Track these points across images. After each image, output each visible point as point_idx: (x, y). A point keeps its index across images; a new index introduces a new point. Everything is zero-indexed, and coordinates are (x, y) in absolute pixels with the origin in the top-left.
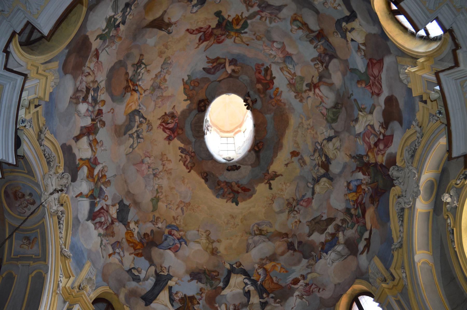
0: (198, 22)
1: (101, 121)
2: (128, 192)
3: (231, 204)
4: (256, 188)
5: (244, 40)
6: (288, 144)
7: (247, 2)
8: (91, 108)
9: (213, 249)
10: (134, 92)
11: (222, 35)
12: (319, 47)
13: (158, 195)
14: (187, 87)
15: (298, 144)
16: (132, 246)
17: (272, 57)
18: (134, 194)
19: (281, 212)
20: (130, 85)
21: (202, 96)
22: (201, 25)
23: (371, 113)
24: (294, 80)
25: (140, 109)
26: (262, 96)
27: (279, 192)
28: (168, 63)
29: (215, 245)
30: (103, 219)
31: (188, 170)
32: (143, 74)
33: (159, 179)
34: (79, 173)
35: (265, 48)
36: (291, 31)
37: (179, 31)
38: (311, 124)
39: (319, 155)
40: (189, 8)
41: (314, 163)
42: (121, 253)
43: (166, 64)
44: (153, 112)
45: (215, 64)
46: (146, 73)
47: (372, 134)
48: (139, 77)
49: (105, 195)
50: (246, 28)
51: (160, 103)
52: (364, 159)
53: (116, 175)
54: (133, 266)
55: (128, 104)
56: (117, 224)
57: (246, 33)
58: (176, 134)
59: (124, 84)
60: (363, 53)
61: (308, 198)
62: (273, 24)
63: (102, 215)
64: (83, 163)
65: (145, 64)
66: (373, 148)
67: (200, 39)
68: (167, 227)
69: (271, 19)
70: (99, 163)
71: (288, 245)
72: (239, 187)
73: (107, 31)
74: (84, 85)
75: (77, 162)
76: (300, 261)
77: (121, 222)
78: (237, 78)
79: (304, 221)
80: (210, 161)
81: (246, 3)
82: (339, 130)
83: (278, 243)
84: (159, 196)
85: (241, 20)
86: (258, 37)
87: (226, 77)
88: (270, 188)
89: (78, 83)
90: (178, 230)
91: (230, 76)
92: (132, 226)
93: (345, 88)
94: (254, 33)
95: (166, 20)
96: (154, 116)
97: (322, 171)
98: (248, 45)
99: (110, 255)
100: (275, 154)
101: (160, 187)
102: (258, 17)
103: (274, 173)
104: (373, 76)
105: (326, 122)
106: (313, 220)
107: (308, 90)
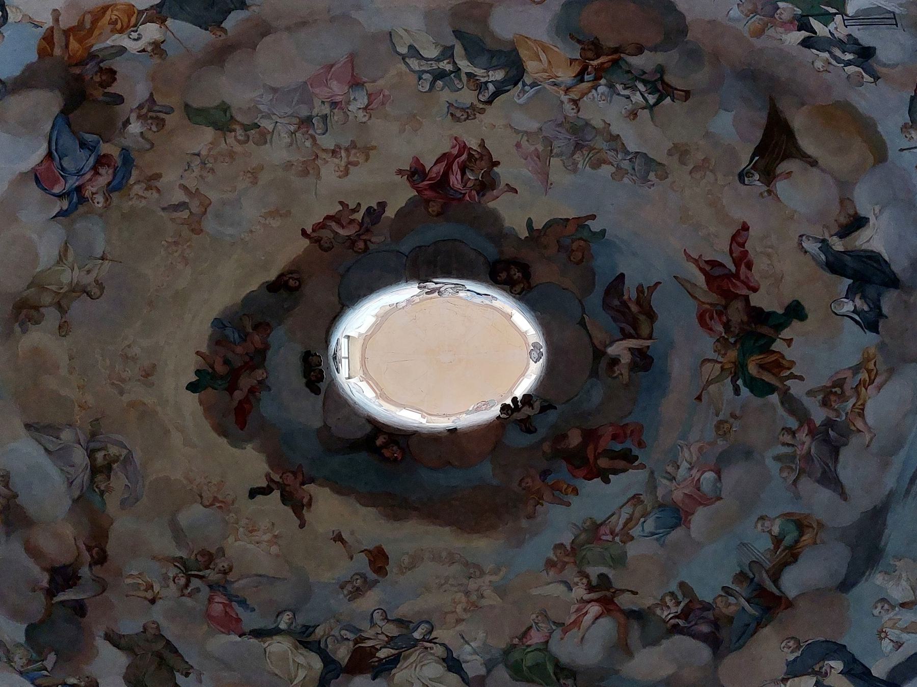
0: (769, 256)
2: (264, 29)
3: (193, 369)
4: (249, 447)
5: (712, 388)
6: (406, 537)
7: (838, 390)
9: (36, 308)
10: (577, 68)
11: (727, 326)
12: (732, 600)
13: (237, 127)
14: (571, 228)
15: (412, 566)
16: (81, 23)
17: (670, 469)
18: (254, 48)
19: (178, 534)
20: (602, 59)
21: (542, 273)
22: (760, 265)
24: (609, 538)
25: (524, 85)
26: (546, 447)
27: (243, 522)
29: (51, 317)
31: (309, 231)
32: (628, 97)
35: (694, 449)
36: (762, 518)
37: (744, 205)
38: (484, 602)
39: (391, 639)
40: (818, 232)
41: (365, 625)
43: (647, 167)
45: (634, 308)
46: (630, 107)
48: (619, 87)
50: (752, 391)
51: (532, 148)
54: (11, 17)
55: (545, 49)
57: (737, 391)
58: (428, 194)
59: (610, 41)
61: (239, 620)
62: (774, 467)
65: (656, 104)
67: (714, 264)
69: (792, 457)
71: (65, 567)
72: (252, 391)
76: (15, 614)
78: (594, 373)
79: (157, 613)
80: (335, 299)
83: (69, 531)
84: (234, 130)
86: (726, 426)
87: (596, 342)
88: (254, 493)
90: (111, 189)
91: (598, 354)
92: (151, 32)
94: (738, 413)
97: (343, 654)
98: (699, 398)
100: (370, 499)
101: (264, 138)
102: (793, 423)
103: (305, 501)
106: (168, 642)
107: (589, 582)
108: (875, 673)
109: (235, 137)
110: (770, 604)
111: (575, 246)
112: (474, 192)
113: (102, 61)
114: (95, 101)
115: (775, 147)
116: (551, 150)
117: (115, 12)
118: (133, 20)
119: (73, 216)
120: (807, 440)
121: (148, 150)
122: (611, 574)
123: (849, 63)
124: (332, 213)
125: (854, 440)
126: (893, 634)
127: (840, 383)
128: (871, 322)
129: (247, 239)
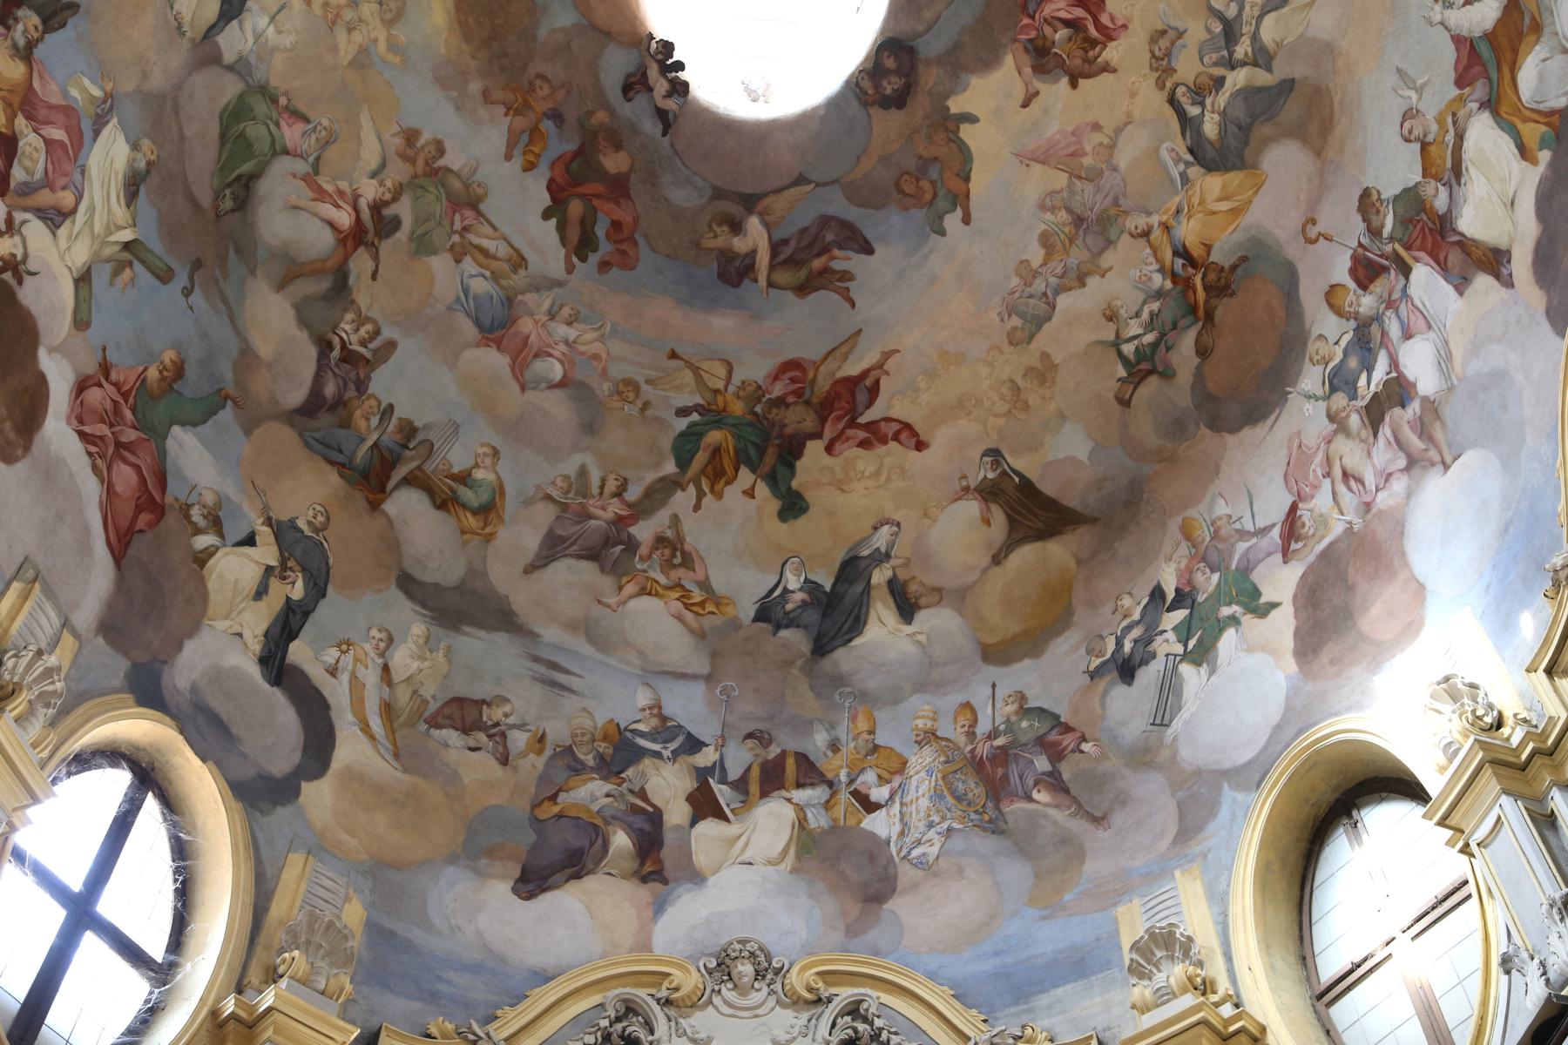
0: (876, 474)
1: (1374, 232)
5: (688, 376)
7: (678, 560)
8: (1394, 329)
10: (1197, 252)
11: (780, 402)
12: (375, 421)
14: (955, 184)
17: (566, 311)
22: (864, 461)
23: (83, 280)
24: (458, 226)
26: (601, 116)
28: (1022, 316)
32: (1138, 315)
35: (597, 347)
37: (954, 450)
40: (901, 550)
43: (1031, 318)
45: (817, 264)
47: (48, 183)
48: (1155, 306)
50: (682, 434)
51: (1088, 148)
52: (35, 20)
55: (1235, 213)
57: (682, 412)
59: (1224, 310)
60: (196, 515)
62: (570, 467)
64: (1526, 120)
65: (1120, 354)
66: (11, 119)
67: (874, 391)
70: (1458, 40)
73: (1226, 611)
75: (1545, 156)
78: (719, 194)
81: (683, 553)
82: (200, 80)
85: (703, 471)
86: (631, 395)
89: (1399, 485)
91: (750, 202)
93: (225, 301)
94: (650, 412)
95: (998, 516)
96: (1133, 95)
98: (674, 355)
102: (633, 494)
104: (129, 447)
105: (273, 82)
107: (386, 204)
108: (293, 646)
110: (373, 479)
111: (925, 184)
112: (1033, 34)
115: (1028, 510)
116: (1080, 178)
120: (609, 514)
122: (402, 235)
123: (1119, 643)
125: (607, 582)
126: (348, 660)
127: (688, 562)
128: (769, 612)
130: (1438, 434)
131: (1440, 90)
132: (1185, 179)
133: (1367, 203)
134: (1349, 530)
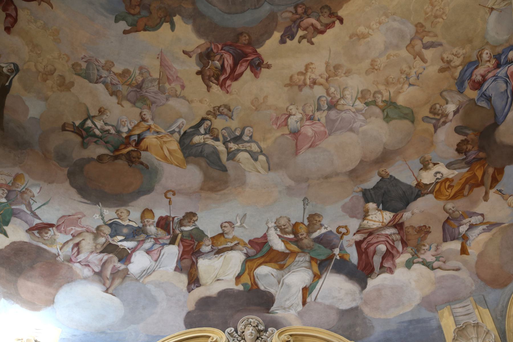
1: (181, 223)
2: (354, 174)
8: (147, 245)
10: (143, 144)
13: (380, 104)
16: (471, 189)
18: (362, 162)
25: (179, 132)
28: (88, 68)
30: (383, 248)
31: (337, 22)
32: (106, 124)
33: (343, 97)
34: (262, 288)
42: (474, 220)
43: (88, 72)
44: (190, 102)
46: (105, 117)
48: (113, 131)
49: (335, 231)
51: (173, 85)
53: (305, 199)
55: (165, 158)
56: (406, 215)
58: (249, 50)
59: (121, 163)
63: (372, 248)
64: (249, 274)
65: (85, 120)
68: (461, 91)
70: (265, 236)
74: (96, 259)
75: (240, 287)
77: (408, 204)
84: (383, 101)
89: (87, 272)
96: (201, 101)
99: (464, 251)
101: (363, 95)
109: (383, 97)
111: (137, 10)
112: (215, 51)
113: (463, 159)
114: (474, 130)
116: (159, 83)
117: (448, 194)
118: (438, 186)
119: (507, 45)
121: (444, 91)
124: (320, 36)
129: (383, 18)
130: (117, 281)
131: (246, 234)
132: (172, 132)
133: (191, 216)
134: (56, 256)
